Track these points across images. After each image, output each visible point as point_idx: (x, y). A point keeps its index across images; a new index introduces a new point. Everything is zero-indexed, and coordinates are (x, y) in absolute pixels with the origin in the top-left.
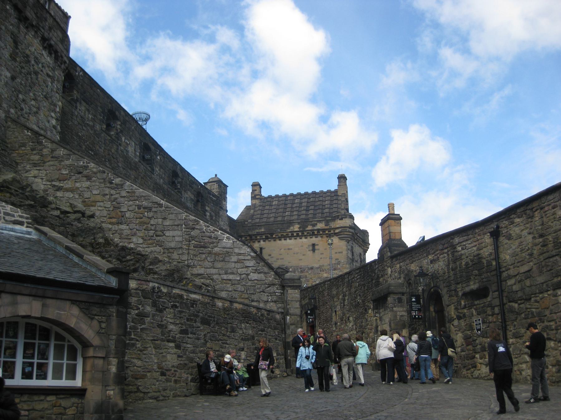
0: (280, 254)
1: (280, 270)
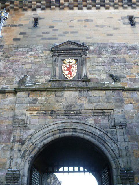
0: (71, 27)
1: (72, 47)
